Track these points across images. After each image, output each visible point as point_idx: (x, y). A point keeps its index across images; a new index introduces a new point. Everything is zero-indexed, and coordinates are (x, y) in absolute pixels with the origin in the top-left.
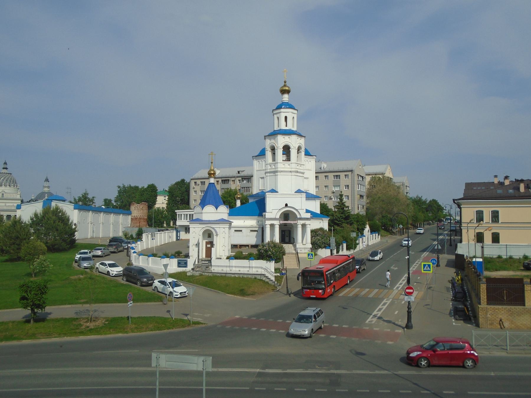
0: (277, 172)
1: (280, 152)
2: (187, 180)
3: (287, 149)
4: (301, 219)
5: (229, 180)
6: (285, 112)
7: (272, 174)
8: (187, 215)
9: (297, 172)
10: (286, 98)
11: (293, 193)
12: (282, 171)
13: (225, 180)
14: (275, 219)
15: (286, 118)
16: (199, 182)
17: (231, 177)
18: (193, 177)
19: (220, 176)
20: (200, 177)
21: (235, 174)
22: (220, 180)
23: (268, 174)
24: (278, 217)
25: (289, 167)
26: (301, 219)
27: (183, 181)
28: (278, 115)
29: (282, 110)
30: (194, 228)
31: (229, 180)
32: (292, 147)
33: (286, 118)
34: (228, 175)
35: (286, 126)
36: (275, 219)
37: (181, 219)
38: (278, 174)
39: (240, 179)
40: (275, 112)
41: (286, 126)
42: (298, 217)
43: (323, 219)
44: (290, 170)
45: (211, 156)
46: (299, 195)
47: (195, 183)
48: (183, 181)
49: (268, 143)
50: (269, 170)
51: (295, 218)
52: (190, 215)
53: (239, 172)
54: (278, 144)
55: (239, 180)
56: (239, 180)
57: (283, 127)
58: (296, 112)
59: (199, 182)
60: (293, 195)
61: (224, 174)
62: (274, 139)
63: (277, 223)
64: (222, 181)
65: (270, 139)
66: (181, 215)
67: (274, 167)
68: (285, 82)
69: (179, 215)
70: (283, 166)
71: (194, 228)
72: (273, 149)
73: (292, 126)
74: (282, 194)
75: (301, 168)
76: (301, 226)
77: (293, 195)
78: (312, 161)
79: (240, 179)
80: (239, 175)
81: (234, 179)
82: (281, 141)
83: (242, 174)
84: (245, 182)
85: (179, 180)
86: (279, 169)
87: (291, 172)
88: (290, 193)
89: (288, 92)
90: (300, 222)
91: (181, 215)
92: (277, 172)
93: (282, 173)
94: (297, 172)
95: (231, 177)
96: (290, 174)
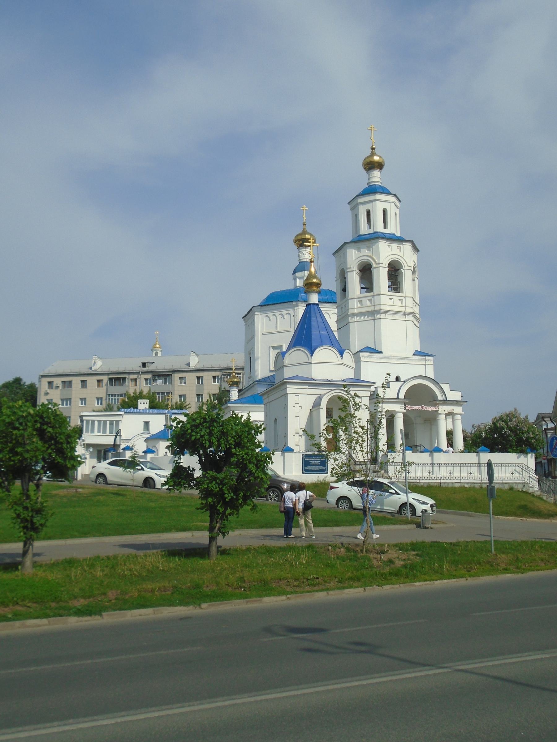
0: (379, 312)
2: (27, 381)
3: (394, 271)
5: (124, 379)
6: (381, 203)
7: (366, 318)
8: (105, 422)
10: (377, 177)
11: (410, 355)
12: (389, 312)
13: (118, 379)
14: (396, 400)
15: (385, 212)
16: (58, 381)
17: (129, 373)
18: (46, 372)
19: (105, 370)
20: (60, 371)
21: (135, 365)
22: (105, 379)
23: (356, 319)
25: (399, 303)
26: (446, 402)
27: (18, 381)
28: (369, 206)
30: (297, 394)
31: (124, 379)
32: (405, 266)
33: (385, 212)
34: (121, 369)
37: (93, 431)
38: (382, 316)
39: (149, 376)
40: (360, 200)
42: (440, 398)
44: (403, 310)
47: (50, 383)
48: (18, 381)
49: (354, 257)
50: (356, 311)
51: (434, 401)
52: (111, 423)
53: (144, 365)
54: (379, 258)
55: (146, 379)
56: (146, 379)
57: (380, 228)
59: (58, 381)
60: (410, 359)
61: (114, 369)
62: (369, 248)
63: (399, 408)
64: (111, 379)
65: (359, 250)
66: (93, 421)
67: (369, 304)
69: (88, 421)
70: (390, 302)
71: (297, 394)
72: (366, 271)
73: (393, 228)
74: (389, 358)
76: (443, 416)
77: (410, 359)
79: (149, 376)
80: (144, 369)
81: (135, 377)
82: (385, 253)
83: (152, 368)
84: (159, 382)
85: (10, 378)
86: (383, 307)
87: (405, 313)
88: (404, 355)
89: (380, 166)
90: (444, 409)
91: (93, 421)
92: (379, 312)
93: (388, 316)
95: (129, 373)
96: (403, 318)
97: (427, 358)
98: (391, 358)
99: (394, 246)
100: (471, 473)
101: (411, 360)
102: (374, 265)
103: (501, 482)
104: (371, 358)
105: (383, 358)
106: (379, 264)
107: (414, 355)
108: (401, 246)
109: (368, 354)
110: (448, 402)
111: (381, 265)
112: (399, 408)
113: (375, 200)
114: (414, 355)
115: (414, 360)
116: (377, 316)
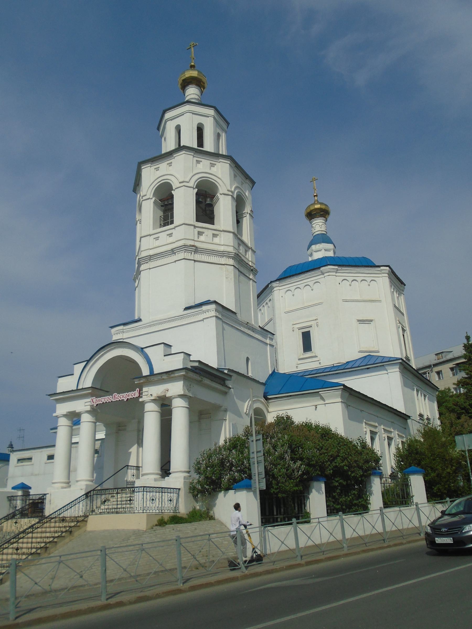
4: (155, 378)
9: (196, 250)
11: (181, 312)
12: (150, 258)
15: (178, 129)
25: (171, 240)
33: (178, 129)
42: (146, 372)
43: (323, 393)
58: (211, 112)
60: (181, 317)
74: (150, 325)
75: (216, 240)
77: (181, 317)
87: (173, 252)
90: (152, 391)
94: (196, 250)
97: (204, 308)
98: (154, 325)
101: (182, 318)
104: (128, 332)
105: (143, 328)
107: (186, 309)
110: (156, 378)
111: (144, 198)
112: (81, 406)
114: (186, 309)
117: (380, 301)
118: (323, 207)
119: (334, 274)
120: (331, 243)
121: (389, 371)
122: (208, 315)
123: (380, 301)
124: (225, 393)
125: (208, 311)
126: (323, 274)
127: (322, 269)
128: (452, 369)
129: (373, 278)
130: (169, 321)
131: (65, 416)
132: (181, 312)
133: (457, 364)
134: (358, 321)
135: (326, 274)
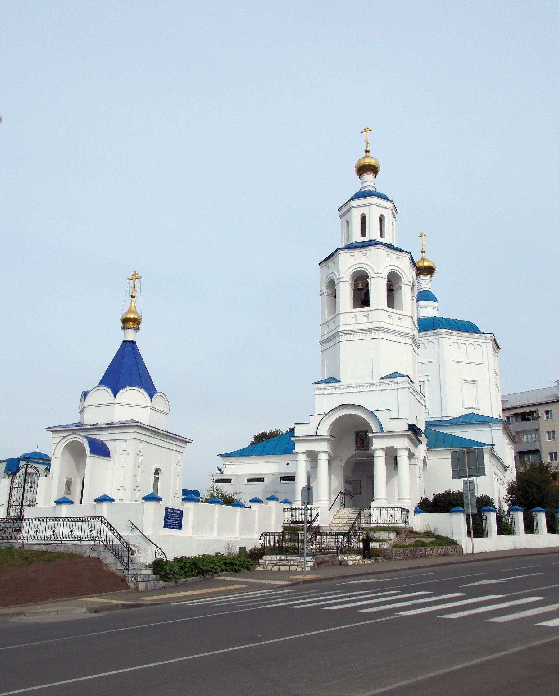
1: (345, 292)
9: (387, 330)
11: (377, 380)
15: (363, 219)
24: (324, 431)
25: (365, 320)
29: (354, 203)
32: (371, 274)
33: (363, 219)
35: (364, 234)
36: (314, 438)
38: (341, 338)
41: (364, 234)
45: (132, 281)
46: (391, 384)
57: (357, 237)
58: (390, 205)
68: (367, 152)
70: (353, 321)
78: (484, 345)
86: (342, 328)
87: (370, 330)
88: (370, 380)
93: (349, 337)
94: (387, 330)
97: (399, 379)
99: (359, 254)
100: (72, 531)
102: (336, 283)
103: (79, 542)
106: (339, 278)
108: (368, 252)
109: (323, 385)
111: (341, 280)
113: (351, 208)
115: (385, 384)
116: (337, 340)
117: (483, 364)
118: (431, 265)
119: (447, 336)
120: (436, 301)
121: (493, 428)
122: (400, 386)
123: (483, 364)
124: (416, 446)
125: (402, 382)
126: (437, 335)
127: (436, 331)
128: (508, 418)
129: (479, 343)
130: (366, 386)
131: (304, 453)
132: (377, 380)
133: (514, 414)
134: (465, 380)
135: (440, 336)
